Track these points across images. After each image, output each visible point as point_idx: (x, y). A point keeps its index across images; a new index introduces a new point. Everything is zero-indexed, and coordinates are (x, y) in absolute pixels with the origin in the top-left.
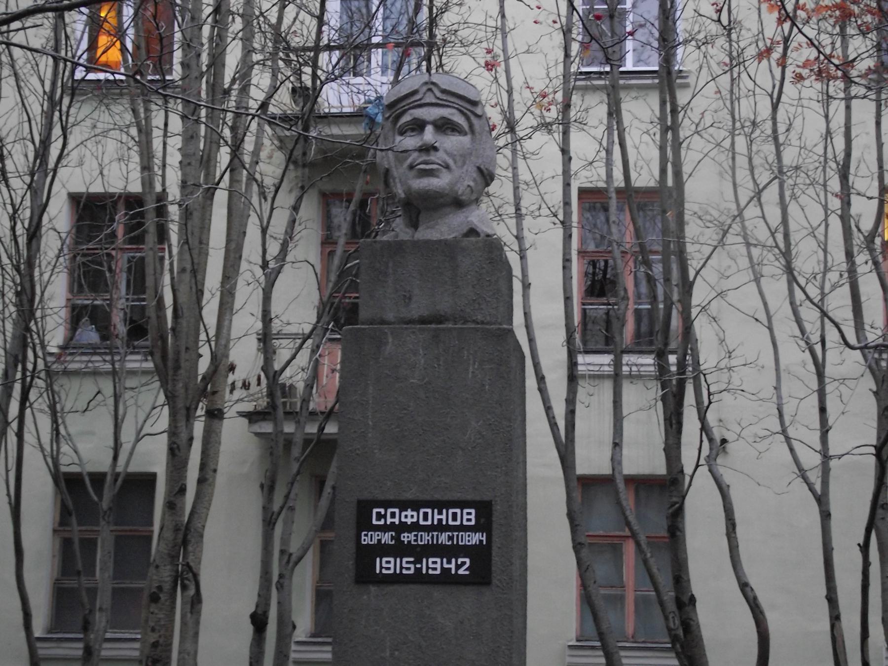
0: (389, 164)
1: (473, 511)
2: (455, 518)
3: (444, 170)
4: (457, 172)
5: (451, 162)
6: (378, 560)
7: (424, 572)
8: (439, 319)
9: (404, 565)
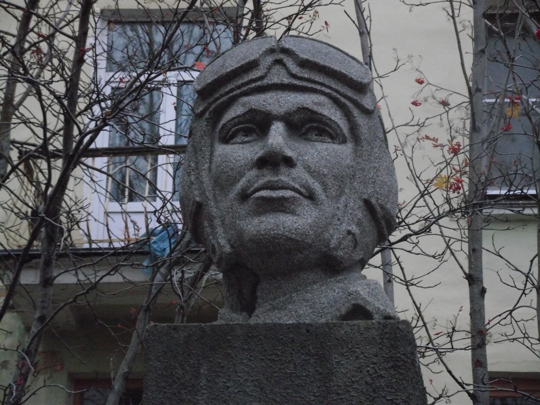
0: (203, 194)
3: (306, 202)
4: (328, 207)
5: (317, 187)
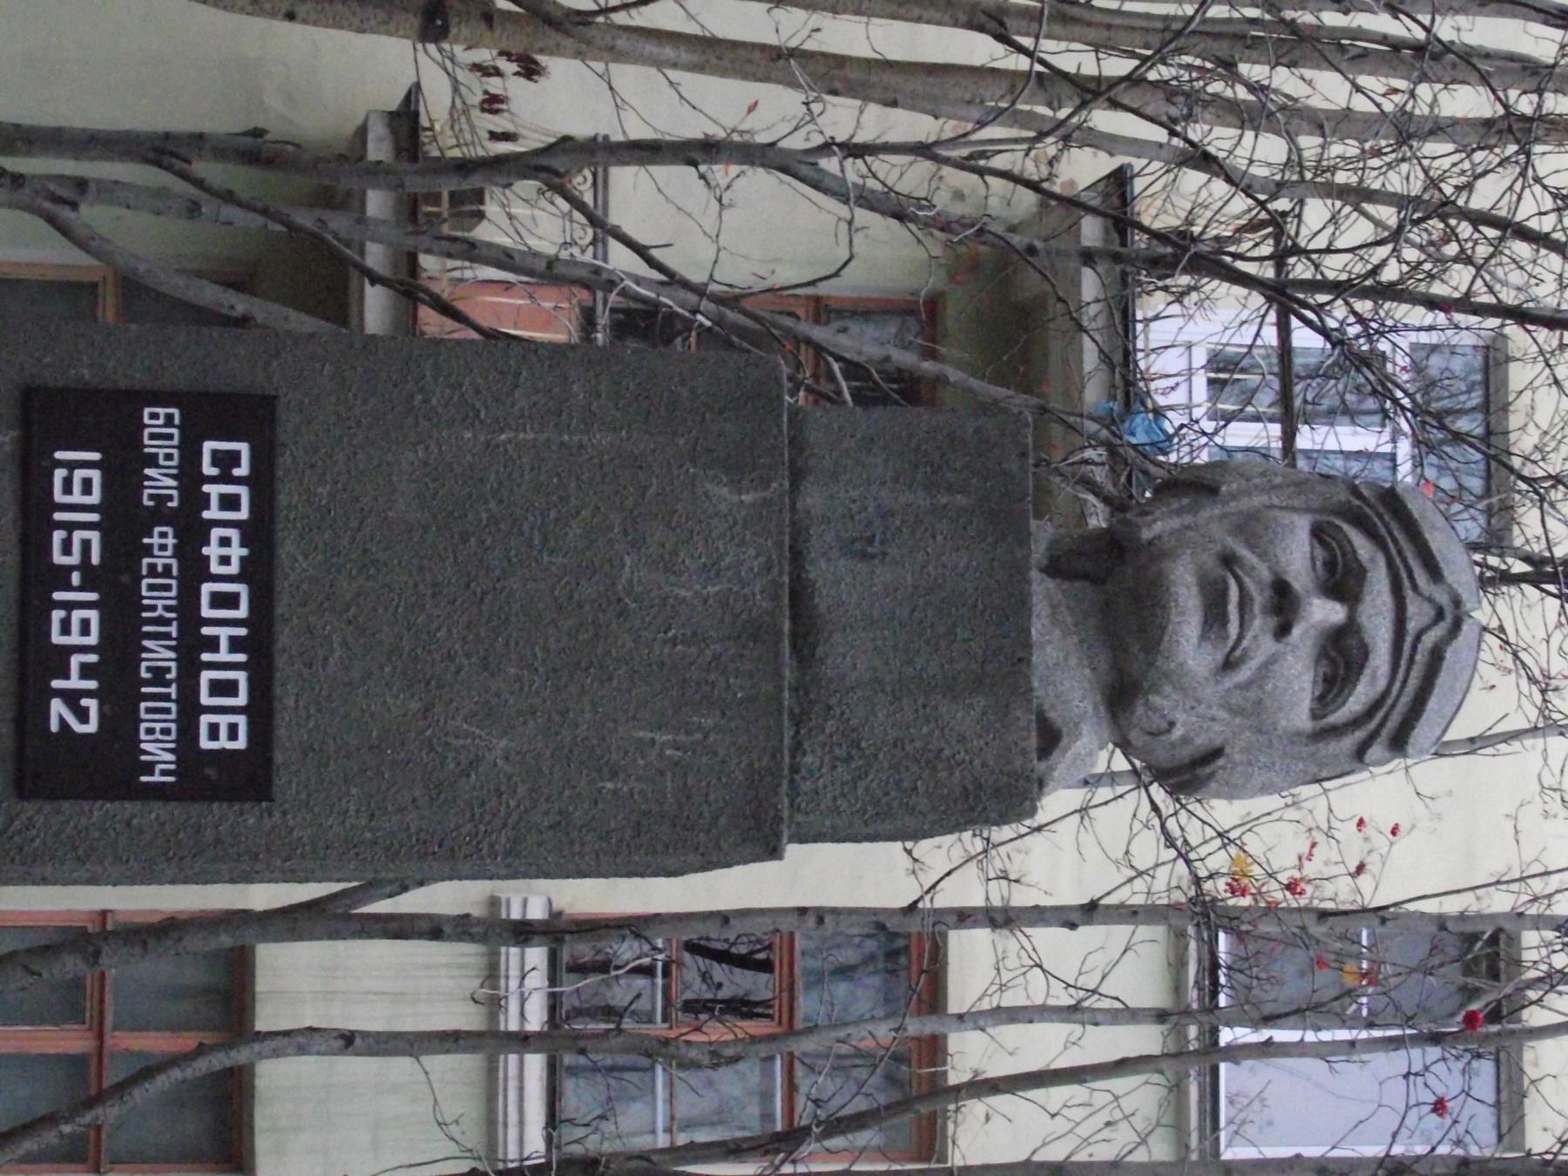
1: (241, 744)
2: (219, 688)
3: (1220, 657)
5: (1244, 674)
6: (95, 456)
7: (58, 596)
8: (806, 633)
9: (78, 536)
